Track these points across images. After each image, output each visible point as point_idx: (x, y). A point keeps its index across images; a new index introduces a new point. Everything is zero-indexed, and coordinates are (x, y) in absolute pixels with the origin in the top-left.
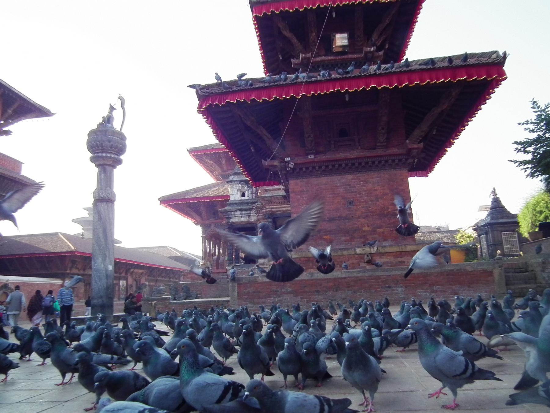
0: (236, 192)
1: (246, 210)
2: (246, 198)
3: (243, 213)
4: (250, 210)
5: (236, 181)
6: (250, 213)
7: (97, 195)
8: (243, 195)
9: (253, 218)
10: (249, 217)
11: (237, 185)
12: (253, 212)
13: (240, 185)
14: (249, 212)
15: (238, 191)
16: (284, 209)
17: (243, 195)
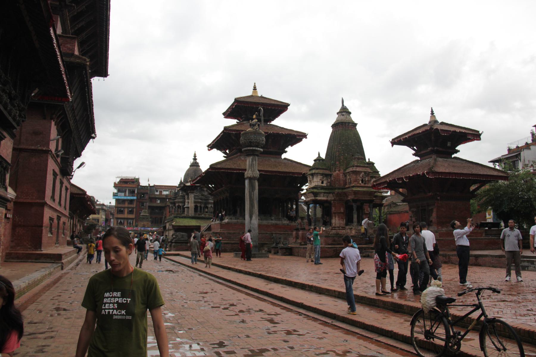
0: (319, 180)
1: (327, 193)
2: (324, 185)
3: (325, 194)
4: (329, 193)
5: (319, 174)
6: (328, 195)
7: (252, 175)
8: (322, 183)
9: (329, 199)
10: (327, 197)
11: (320, 176)
12: (331, 195)
13: (322, 177)
14: (328, 194)
15: (320, 180)
16: (364, 198)
17: (322, 183)
